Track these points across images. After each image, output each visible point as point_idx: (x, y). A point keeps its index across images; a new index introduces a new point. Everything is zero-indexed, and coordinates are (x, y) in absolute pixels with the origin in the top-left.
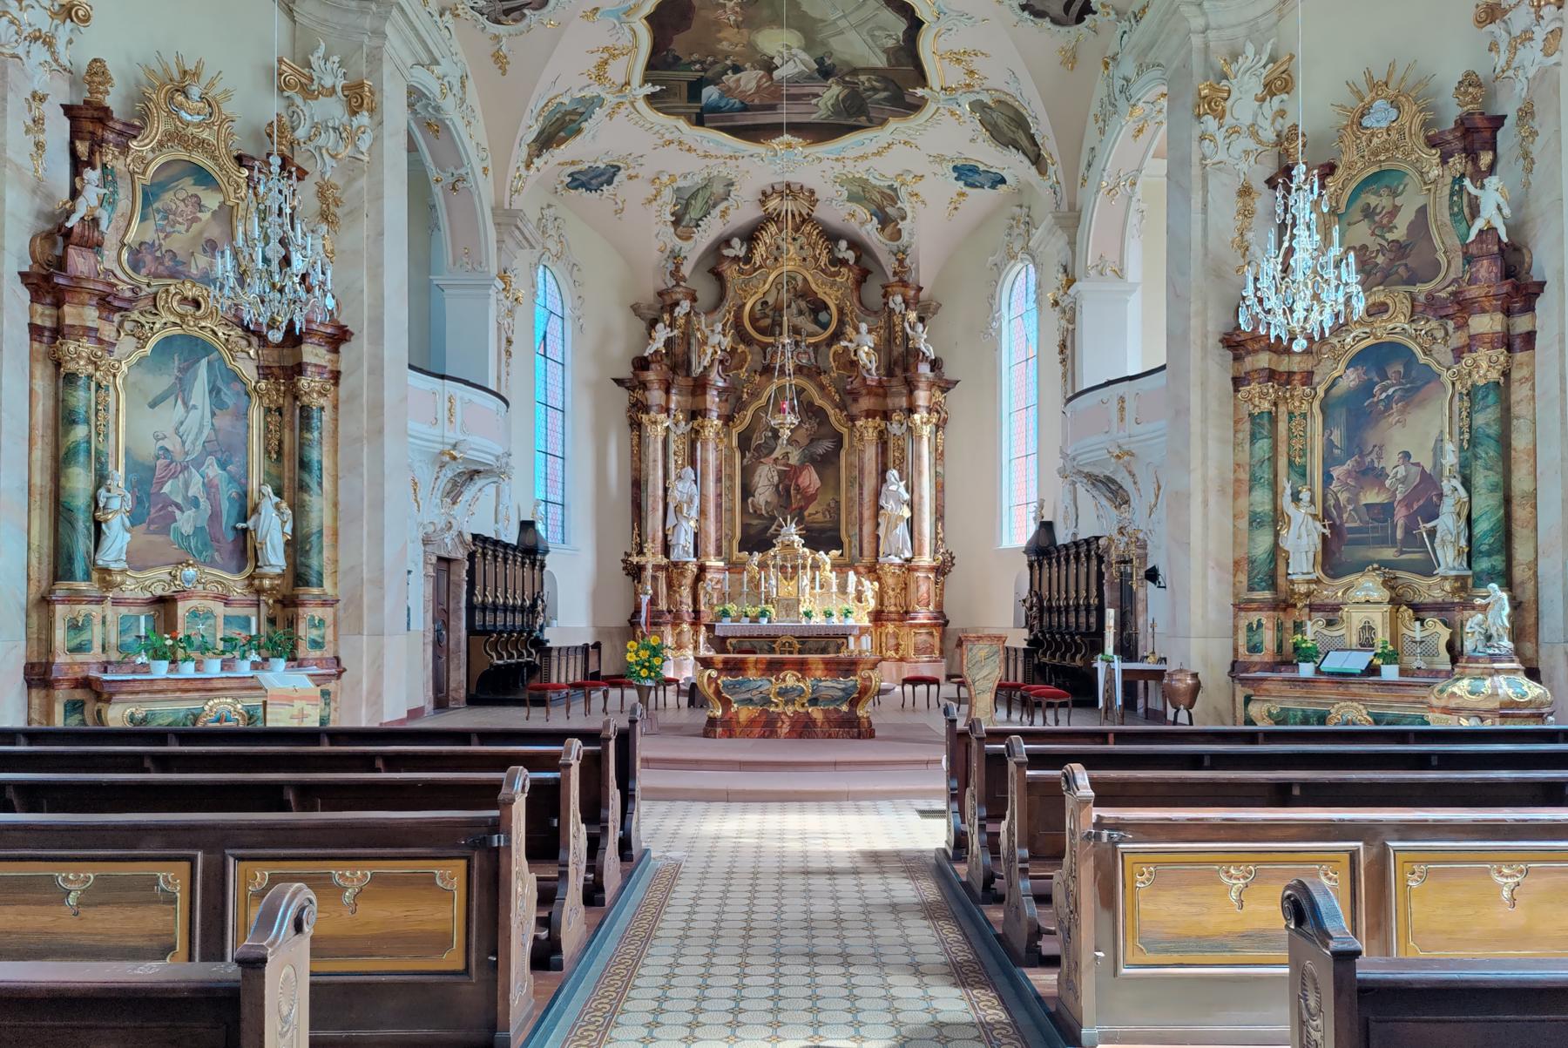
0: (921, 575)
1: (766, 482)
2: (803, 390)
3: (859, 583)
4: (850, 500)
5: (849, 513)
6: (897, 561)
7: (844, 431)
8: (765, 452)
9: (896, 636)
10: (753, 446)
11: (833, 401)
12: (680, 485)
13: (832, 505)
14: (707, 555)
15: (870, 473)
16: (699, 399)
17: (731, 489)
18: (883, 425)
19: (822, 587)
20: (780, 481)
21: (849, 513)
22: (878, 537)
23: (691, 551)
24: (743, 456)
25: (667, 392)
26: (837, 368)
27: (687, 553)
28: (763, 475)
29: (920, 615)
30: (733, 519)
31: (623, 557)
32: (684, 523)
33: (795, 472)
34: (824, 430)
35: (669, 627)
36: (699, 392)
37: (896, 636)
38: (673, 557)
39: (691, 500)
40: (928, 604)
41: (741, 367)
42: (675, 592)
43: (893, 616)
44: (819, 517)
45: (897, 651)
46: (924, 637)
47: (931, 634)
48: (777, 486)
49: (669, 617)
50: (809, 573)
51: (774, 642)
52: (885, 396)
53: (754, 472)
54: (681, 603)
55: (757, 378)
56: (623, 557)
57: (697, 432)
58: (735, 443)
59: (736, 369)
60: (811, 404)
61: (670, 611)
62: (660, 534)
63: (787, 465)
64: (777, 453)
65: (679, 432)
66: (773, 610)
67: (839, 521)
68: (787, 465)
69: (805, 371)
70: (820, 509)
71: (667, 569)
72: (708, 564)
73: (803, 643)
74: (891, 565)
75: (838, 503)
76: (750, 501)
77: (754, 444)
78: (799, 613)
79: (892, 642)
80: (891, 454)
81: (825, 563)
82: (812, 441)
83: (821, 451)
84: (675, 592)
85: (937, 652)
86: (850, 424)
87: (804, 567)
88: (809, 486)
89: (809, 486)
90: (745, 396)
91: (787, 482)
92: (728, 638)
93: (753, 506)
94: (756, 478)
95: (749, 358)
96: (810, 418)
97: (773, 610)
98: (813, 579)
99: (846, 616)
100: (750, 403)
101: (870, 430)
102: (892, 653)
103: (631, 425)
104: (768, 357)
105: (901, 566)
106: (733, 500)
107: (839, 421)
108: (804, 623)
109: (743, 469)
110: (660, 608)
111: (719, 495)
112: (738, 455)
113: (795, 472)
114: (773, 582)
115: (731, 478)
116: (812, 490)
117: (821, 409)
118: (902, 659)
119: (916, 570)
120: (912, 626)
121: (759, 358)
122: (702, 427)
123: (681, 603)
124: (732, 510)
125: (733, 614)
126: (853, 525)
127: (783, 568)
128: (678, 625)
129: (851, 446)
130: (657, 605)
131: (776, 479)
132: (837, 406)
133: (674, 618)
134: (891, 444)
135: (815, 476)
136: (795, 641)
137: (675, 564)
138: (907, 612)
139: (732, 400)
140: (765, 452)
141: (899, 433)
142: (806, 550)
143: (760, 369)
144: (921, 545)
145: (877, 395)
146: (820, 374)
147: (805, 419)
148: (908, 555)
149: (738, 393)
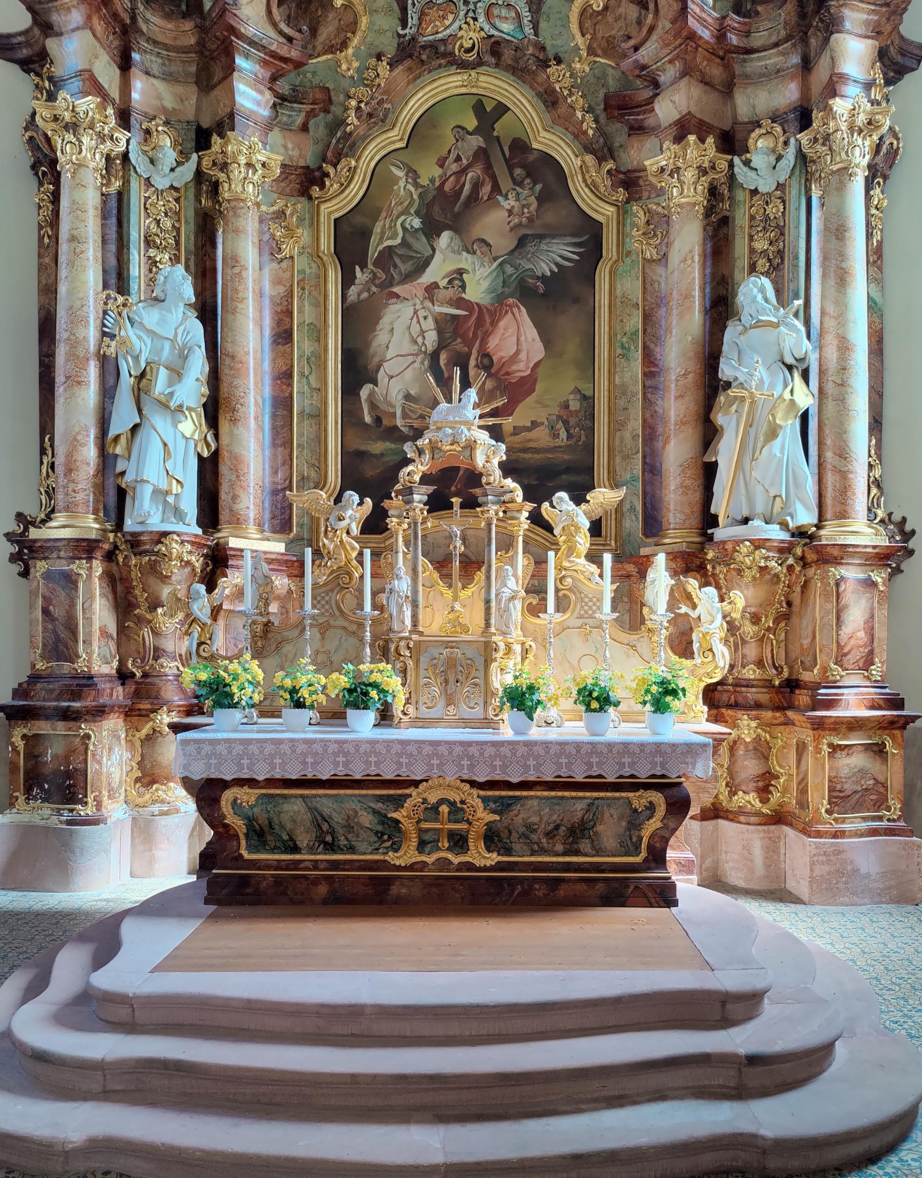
0: (851, 573)
1: (407, 348)
2: (501, 109)
3: (680, 596)
4: (617, 392)
5: (616, 426)
6: (776, 533)
7: (604, 212)
8: (404, 267)
9: (762, 750)
10: (373, 252)
11: (578, 135)
12: (151, 317)
13: (574, 405)
14: (237, 521)
15: (688, 296)
16: (216, 92)
17: (318, 361)
18: (723, 165)
19: (561, 606)
20: (442, 345)
21: (616, 426)
22: (709, 471)
23: (190, 503)
24: (348, 280)
25: (125, 64)
26: (591, 51)
27: (178, 514)
28: (399, 327)
29: (849, 695)
30: (320, 439)
31: (12, 526)
32: (159, 422)
33: (480, 323)
34: (551, 216)
35: (114, 724)
36: (218, 74)
37: (762, 750)
38: (130, 525)
39: (184, 356)
40: (869, 662)
41: (344, 45)
42: (140, 620)
43: (752, 694)
44: (541, 437)
45: (764, 792)
46: (856, 761)
47: (879, 751)
48: (434, 356)
49: (119, 694)
50: (521, 560)
51: (399, 802)
52: (727, 89)
53: (377, 319)
54: (158, 653)
55: (383, 68)
56: (12, 526)
57: (215, 187)
58: (326, 243)
59: (331, 49)
60: (520, 146)
61: (123, 676)
62: (90, 453)
63: (460, 303)
64: (436, 272)
65: (161, 182)
66: (394, 683)
67: (590, 448)
68: (460, 303)
69: (508, 54)
70: (542, 416)
71: (110, 557)
72: (234, 543)
73: (503, 807)
74: (758, 544)
75: (588, 401)
76: (364, 392)
77: (375, 248)
78: (488, 693)
79: (750, 767)
80: (741, 248)
81: (571, 529)
82: (522, 242)
83: (545, 268)
84: (140, 620)
85: (895, 805)
86: (621, 194)
87: (507, 544)
88: (514, 358)
89: (514, 358)
90: (352, 118)
91: (459, 345)
92: (223, 785)
93: (373, 406)
94: (381, 337)
95: (364, 21)
96: (520, 184)
97: (394, 683)
98: (536, 588)
99: (659, 707)
100: (366, 138)
101: (689, 175)
102: (748, 799)
103: (34, 167)
104: (413, 20)
105: (784, 550)
106: (321, 390)
107: (593, 187)
108: (507, 733)
109: (349, 314)
110: (81, 665)
111: (284, 377)
112: (334, 277)
113: (480, 323)
114: (403, 585)
115: (318, 333)
116: (522, 369)
117: (548, 160)
118: (779, 818)
119: (837, 561)
120: (819, 725)
121: (390, 23)
122: (224, 167)
123: (158, 653)
124: (318, 416)
125: (245, 693)
126: (626, 457)
127: (442, 564)
128: (145, 715)
129: (623, 253)
130: (72, 657)
131: (432, 338)
132: (588, 148)
133: (138, 695)
134: (741, 219)
135: (530, 332)
136: (474, 798)
137: (135, 542)
138: (792, 684)
139: (318, 126)
140: (404, 267)
141: (766, 185)
142: (509, 483)
143: (390, 48)
144: (844, 490)
145: (706, 82)
146: (545, 64)
147: (505, 183)
148: (805, 517)
149: (336, 109)
